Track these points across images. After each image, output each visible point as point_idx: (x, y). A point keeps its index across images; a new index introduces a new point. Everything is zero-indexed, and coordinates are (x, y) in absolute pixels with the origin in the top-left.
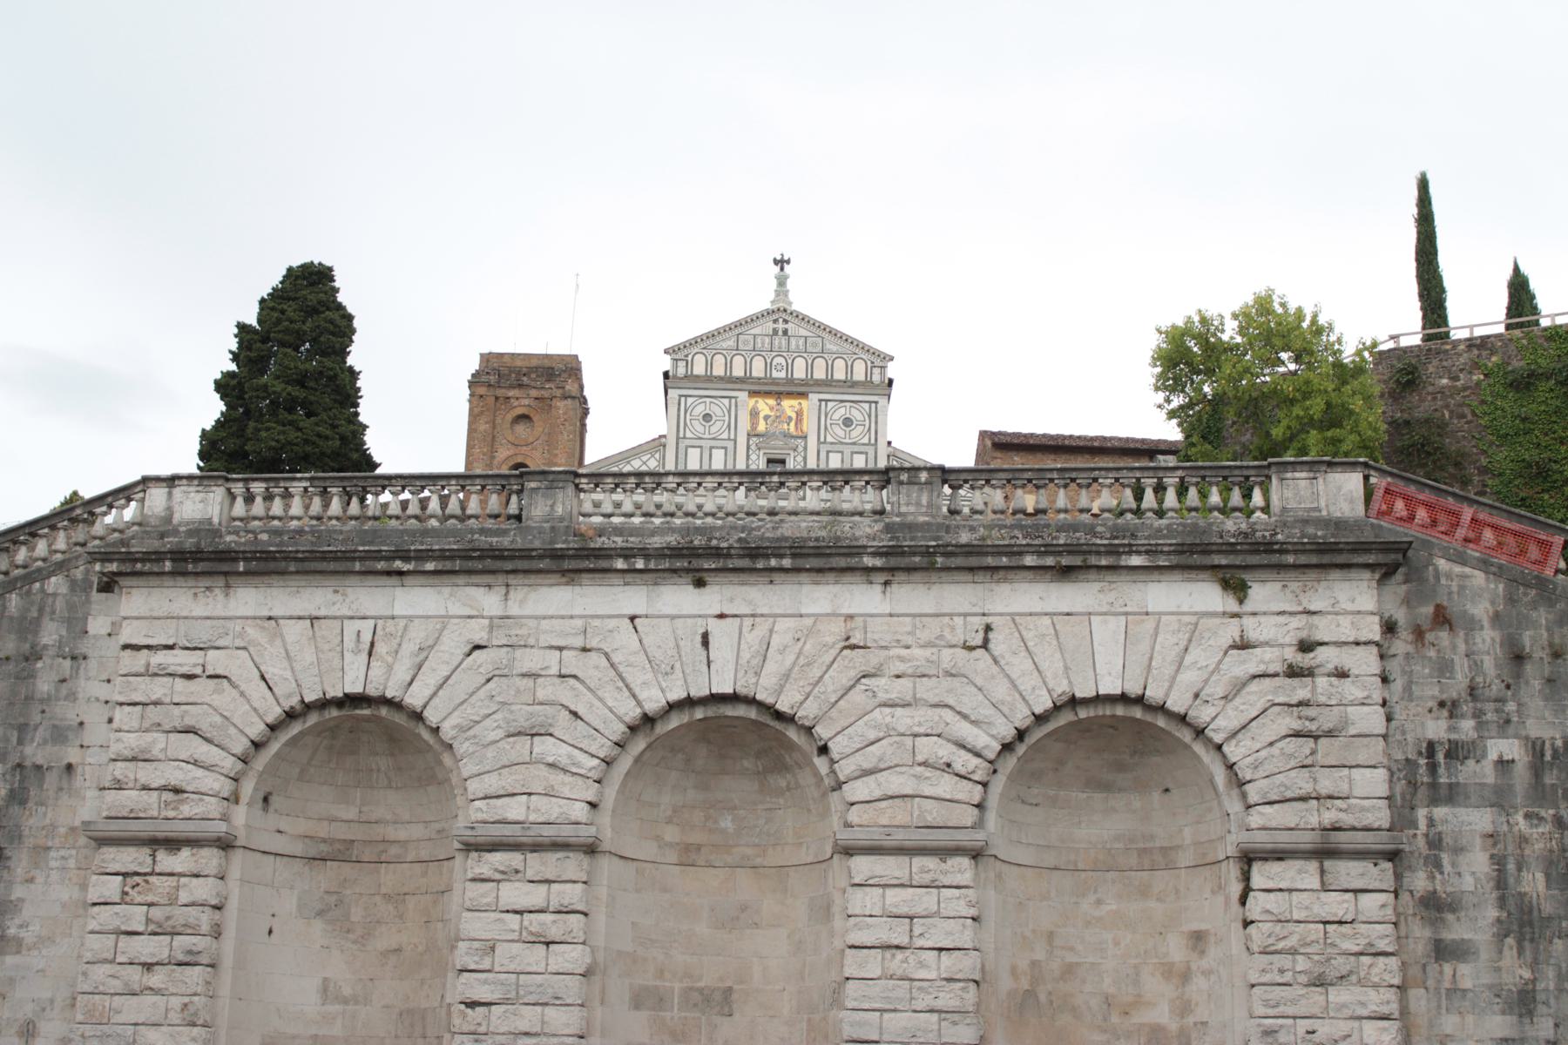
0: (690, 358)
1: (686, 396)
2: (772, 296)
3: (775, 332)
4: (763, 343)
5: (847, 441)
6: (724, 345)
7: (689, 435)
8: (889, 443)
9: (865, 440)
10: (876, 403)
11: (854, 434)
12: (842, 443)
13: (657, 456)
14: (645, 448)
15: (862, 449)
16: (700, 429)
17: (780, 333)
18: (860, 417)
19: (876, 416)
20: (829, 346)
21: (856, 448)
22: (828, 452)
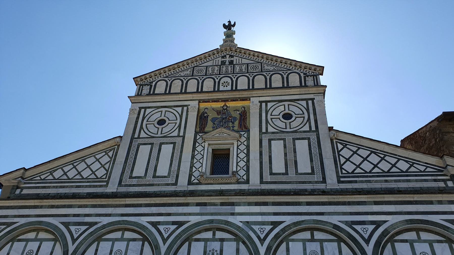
1: (146, 108)
2: (222, 43)
3: (223, 63)
4: (213, 71)
5: (288, 130)
6: (182, 74)
7: (143, 135)
8: (331, 129)
9: (306, 128)
10: (313, 100)
11: (294, 124)
13: (110, 154)
14: (100, 147)
15: (304, 135)
16: (154, 130)
17: (227, 63)
18: (298, 111)
19: (314, 110)
20: (266, 67)
21: (297, 135)
22: (270, 141)
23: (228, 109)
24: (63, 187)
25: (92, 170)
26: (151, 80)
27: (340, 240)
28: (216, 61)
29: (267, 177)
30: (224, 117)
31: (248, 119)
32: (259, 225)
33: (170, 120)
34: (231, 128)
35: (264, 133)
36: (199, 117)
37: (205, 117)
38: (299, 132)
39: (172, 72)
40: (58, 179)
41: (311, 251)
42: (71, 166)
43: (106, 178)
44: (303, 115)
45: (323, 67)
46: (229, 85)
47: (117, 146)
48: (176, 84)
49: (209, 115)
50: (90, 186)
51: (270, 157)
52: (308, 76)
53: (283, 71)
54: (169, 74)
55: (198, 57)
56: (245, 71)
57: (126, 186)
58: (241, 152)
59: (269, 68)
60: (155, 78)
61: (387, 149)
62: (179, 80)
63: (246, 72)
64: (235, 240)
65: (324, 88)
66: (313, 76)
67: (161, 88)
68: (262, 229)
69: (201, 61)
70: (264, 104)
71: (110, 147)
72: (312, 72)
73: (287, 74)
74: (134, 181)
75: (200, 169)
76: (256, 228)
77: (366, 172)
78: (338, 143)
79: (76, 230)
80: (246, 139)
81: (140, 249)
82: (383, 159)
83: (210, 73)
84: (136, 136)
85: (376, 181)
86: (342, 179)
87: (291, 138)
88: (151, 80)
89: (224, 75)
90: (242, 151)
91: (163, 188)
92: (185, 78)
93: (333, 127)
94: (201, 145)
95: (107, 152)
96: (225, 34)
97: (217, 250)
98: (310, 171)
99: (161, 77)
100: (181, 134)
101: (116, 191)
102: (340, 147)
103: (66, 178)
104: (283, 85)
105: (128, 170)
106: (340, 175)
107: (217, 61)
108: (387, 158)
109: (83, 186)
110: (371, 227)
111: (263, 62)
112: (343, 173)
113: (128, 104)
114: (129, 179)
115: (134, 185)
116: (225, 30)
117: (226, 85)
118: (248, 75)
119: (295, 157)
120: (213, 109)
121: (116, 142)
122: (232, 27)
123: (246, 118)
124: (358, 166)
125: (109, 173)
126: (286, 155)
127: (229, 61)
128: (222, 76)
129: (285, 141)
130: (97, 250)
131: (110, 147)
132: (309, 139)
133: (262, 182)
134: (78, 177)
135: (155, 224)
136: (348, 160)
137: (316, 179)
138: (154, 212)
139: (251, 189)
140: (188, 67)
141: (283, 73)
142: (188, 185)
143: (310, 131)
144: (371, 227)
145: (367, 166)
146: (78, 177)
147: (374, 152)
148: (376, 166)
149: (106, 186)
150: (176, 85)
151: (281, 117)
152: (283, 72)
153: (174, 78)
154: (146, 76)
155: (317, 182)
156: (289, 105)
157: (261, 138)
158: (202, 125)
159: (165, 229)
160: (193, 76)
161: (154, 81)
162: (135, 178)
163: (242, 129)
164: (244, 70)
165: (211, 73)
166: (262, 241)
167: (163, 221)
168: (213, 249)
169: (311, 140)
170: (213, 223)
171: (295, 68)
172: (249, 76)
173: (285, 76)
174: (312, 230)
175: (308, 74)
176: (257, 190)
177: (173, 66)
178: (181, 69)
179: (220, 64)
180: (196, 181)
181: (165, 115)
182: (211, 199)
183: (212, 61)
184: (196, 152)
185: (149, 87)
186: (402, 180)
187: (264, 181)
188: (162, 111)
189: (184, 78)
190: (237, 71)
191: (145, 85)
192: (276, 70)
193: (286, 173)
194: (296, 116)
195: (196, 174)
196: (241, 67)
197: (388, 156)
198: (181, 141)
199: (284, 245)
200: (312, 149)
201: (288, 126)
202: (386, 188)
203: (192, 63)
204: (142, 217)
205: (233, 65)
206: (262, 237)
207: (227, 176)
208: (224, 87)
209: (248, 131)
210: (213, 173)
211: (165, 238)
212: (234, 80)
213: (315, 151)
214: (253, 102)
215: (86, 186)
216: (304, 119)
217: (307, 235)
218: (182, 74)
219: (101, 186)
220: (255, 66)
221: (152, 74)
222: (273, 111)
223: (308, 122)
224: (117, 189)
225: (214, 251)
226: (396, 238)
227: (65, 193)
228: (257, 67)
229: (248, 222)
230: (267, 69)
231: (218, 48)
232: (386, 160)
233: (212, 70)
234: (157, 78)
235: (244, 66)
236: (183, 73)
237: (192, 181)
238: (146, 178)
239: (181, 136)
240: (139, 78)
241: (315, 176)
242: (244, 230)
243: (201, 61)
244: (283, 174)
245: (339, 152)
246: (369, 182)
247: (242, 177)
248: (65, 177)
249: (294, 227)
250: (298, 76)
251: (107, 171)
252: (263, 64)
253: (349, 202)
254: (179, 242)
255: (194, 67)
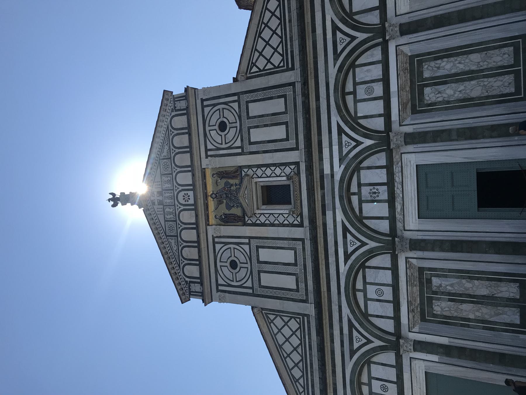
0: (187, 279)
1: (218, 285)
4: (170, 213)
5: (238, 125)
6: (175, 248)
7: (249, 284)
8: (235, 80)
9: (235, 105)
10: (202, 100)
11: (231, 119)
12: (241, 130)
13: (272, 317)
14: (265, 330)
15: (244, 107)
16: (243, 271)
18: (216, 115)
21: (244, 114)
22: (251, 143)
23: (215, 193)
24: (311, 364)
25: (292, 335)
26: (183, 283)
27: (353, 66)
28: (158, 211)
29: (292, 143)
30: (224, 196)
31: (227, 169)
32: (342, 148)
33: (231, 255)
34: (238, 187)
35: (243, 150)
36: (226, 224)
37: (225, 217)
38: (240, 113)
39: (173, 260)
40: (303, 372)
41: (365, 93)
42: (288, 359)
43: (300, 318)
44: (221, 110)
45: (164, 91)
46: (187, 194)
47: (263, 311)
48: (188, 255)
49: (224, 213)
50: (309, 334)
51: (269, 142)
52: (175, 107)
53: (169, 134)
54: (176, 264)
55: (154, 232)
56: (170, 177)
57: (307, 294)
58: (265, 173)
59: (165, 150)
60: (181, 279)
61: (256, 21)
62: (183, 251)
63: (171, 175)
64: (359, 172)
65: (190, 90)
66: (174, 101)
67: (193, 271)
68: (346, 144)
69: (159, 228)
70: (209, 153)
71: (264, 319)
72: (170, 103)
73: (173, 130)
74: (302, 286)
75: (286, 216)
76: (345, 151)
77: (281, 42)
78: (251, 72)
79: (357, 342)
80: (250, 169)
81: (374, 270)
82: (266, 25)
83: (173, 217)
84: (250, 291)
85: (291, 31)
86: (290, 66)
87: (247, 121)
88: (183, 283)
89: (176, 200)
90: (264, 172)
91: (308, 254)
92: (180, 245)
93: (233, 78)
94: (259, 218)
95: (270, 321)
96: (124, 204)
97: (370, 189)
98: (283, 99)
99: (179, 272)
100: (247, 241)
101: (313, 305)
102: (255, 69)
103: (301, 363)
104: (186, 133)
105: (289, 295)
106: (285, 68)
107: (159, 210)
108: (265, 21)
109: (310, 343)
110: (339, 35)
111: (159, 158)
112: (283, 65)
113: (214, 305)
114: (299, 292)
115: (306, 286)
116: (120, 204)
117: (187, 197)
118: (175, 173)
119: (268, 115)
120: (216, 210)
121: (258, 312)
122: (116, 197)
123: (225, 171)
124: (275, 50)
125: (294, 315)
126: (266, 126)
127: (158, 196)
128: (176, 203)
129: (251, 127)
130: (377, 316)
131: (264, 319)
132: (248, 102)
133: (297, 149)
134: (299, 350)
135: (347, 257)
136: (269, 61)
137: (291, 93)
138: (334, 259)
139: (305, 160)
140: (166, 243)
141: (171, 134)
142: (303, 227)
143: (238, 101)
144: (339, 35)
145: (275, 41)
146: (299, 350)
147: (259, 34)
148: (274, 32)
149: (308, 316)
150: (189, 254)
151: (223, 134)
152: (170, 135)
153: (181, 257)
154: (178, 289)
155: (294, 92)
156: (209, 126)
157: (248, 153)
158: (235, 219)
159: (351, 245)
160: (177, 236)
161: (185, 279)
162: (297, 285)
163: (239, 174)
164: (169, 179)
165: (173, 216)
166: (359, 143)
167: (343, 249)
168: (369, 193)
169: (248, 100)
170: (343, 196)
171: (165, 121)
172: (176, 172)
173: (176, 132)
174: (344, 94)
175: (172, 107)
176: (306, 152)
177: (166, 259)
178: (168, 250)
179: (162, 206)
180: (299, 219)
181: (225, 262)
182: (318, 200)
183: (158, 215)
184: (267, 222)
185: (192, 285)
186: (288, 5)
187: (295, 147)
188: (221, 266)
189: (180, 245)
190: (170, 186)
191: (190, 289)
192: (168, 143)
193: (286, 123)
194: (221, 117)
195: (291, 219)
196: (165, 182)
197: (263, 19)
198: (255, 240)
199: (361, 121)
200: (258, 98)
201: (234, 125)
202: (297, 21)
203: (162, 239)
204: (340, 271)
205: (164, 191)
206: (354, 144)
207: (291, 186)
208: (189, 199)
209: (241, 168)
210: (290, 203)
211: (360, 244)
212: (181, 188)
213: (260, 95)
214: (206, 165)
215: (310, 338)
216: (225, 109)
217: (350, 99)
218: (175, 249)
219: (309, 322)
220: (163, 167)
221: (176, 283)
222: (217, 143)
223: (229, 104)
224: (311, 304)
225: (371, 192)
226: (348, 11)
227: (318, 360)
228: (165, 164)
229: (340, 160)
230: (167, 153)
231: (143, 210)
232: (268, 22)
233: (169, 215)
234: (181, 277)
235: (164, 179)
236: (174, 248)
237: (299, 223)
238: (298, 274)
239: (249, 241)
240: (182, 297)
241: (287, 94)
242: (348, 162)
243: (158, 229)
244: (287, 127)
245: (260, 70)
246: (291, 38)
247: (293, 170)
248: (300, 365)
249: (343, 112)
250: (175, 118)
251: (291, 318)
252: (161, 158)
253: (314, 58)
254: (364, 229)
255: (167, 236)
